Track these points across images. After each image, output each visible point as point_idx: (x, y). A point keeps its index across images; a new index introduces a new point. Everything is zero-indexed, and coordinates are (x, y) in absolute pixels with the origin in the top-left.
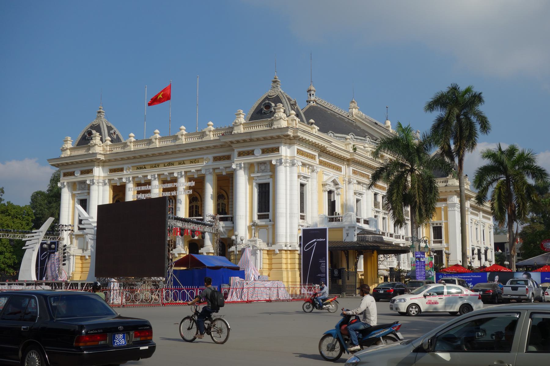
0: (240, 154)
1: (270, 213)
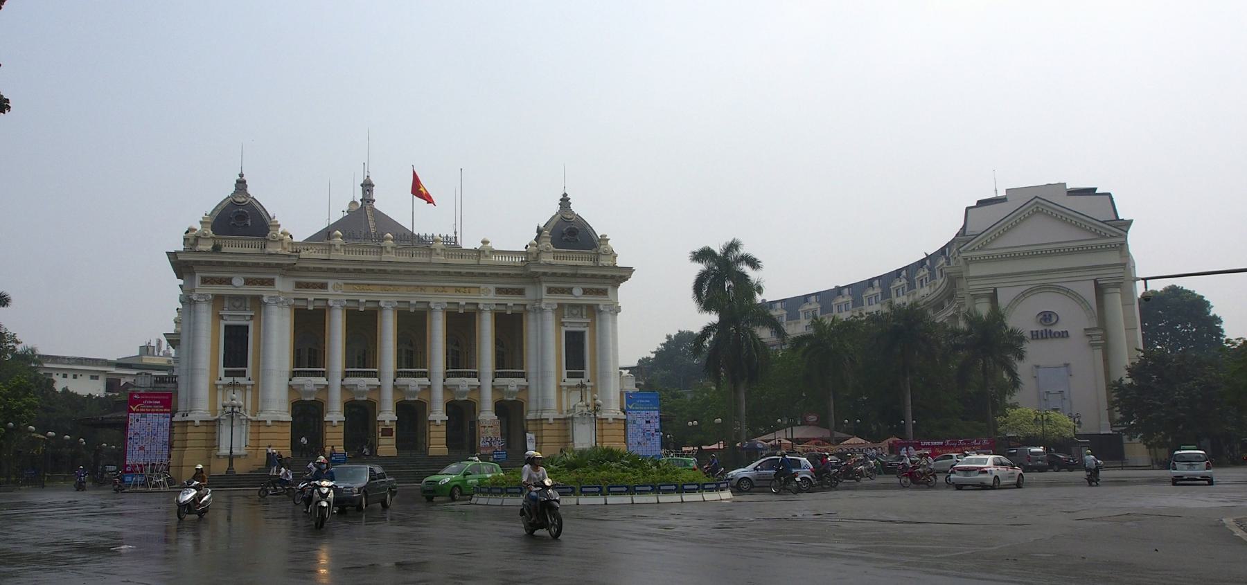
0: (550, 291)
1: (587, 372)
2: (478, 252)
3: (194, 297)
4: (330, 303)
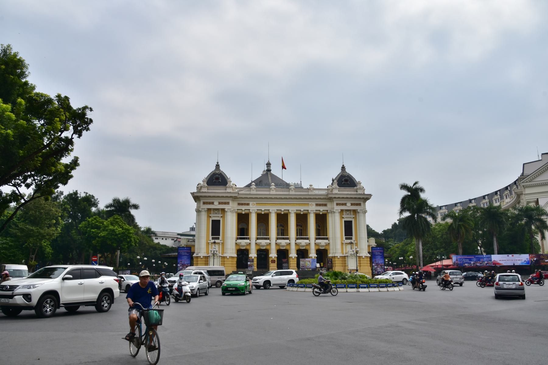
0: (337, 204)
1: (354, 237)
2: (308, 189)
3: (200, 209)
4: (251, 211)
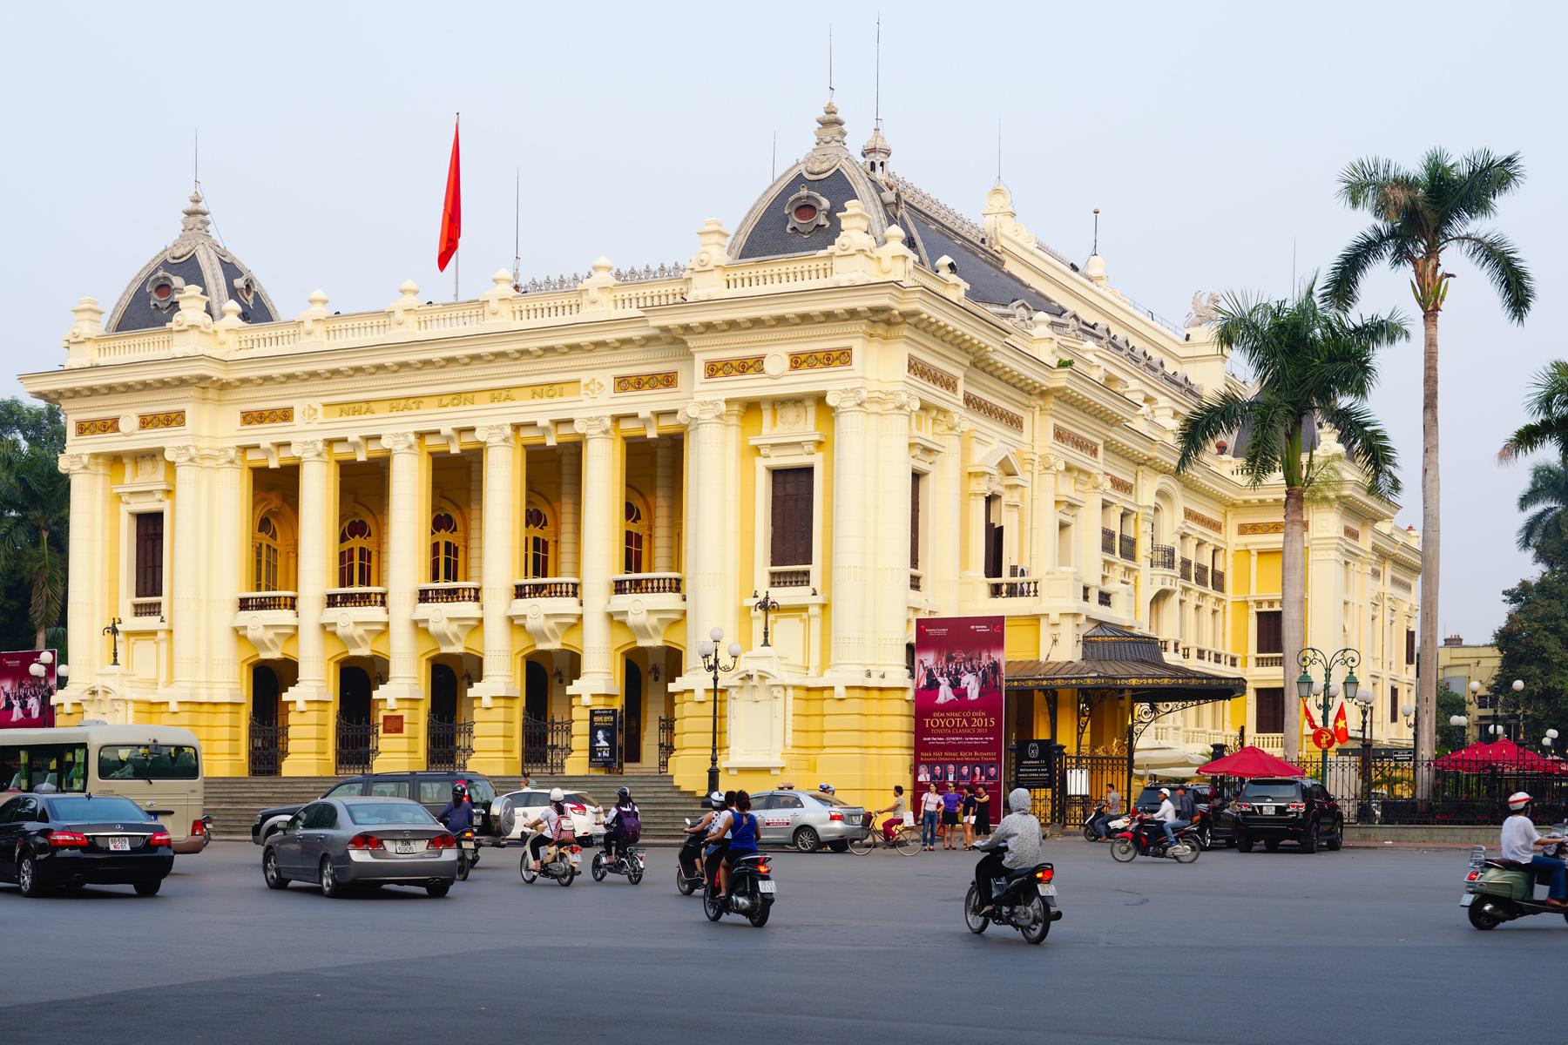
0: (713, 370)
1: (815, 569)
